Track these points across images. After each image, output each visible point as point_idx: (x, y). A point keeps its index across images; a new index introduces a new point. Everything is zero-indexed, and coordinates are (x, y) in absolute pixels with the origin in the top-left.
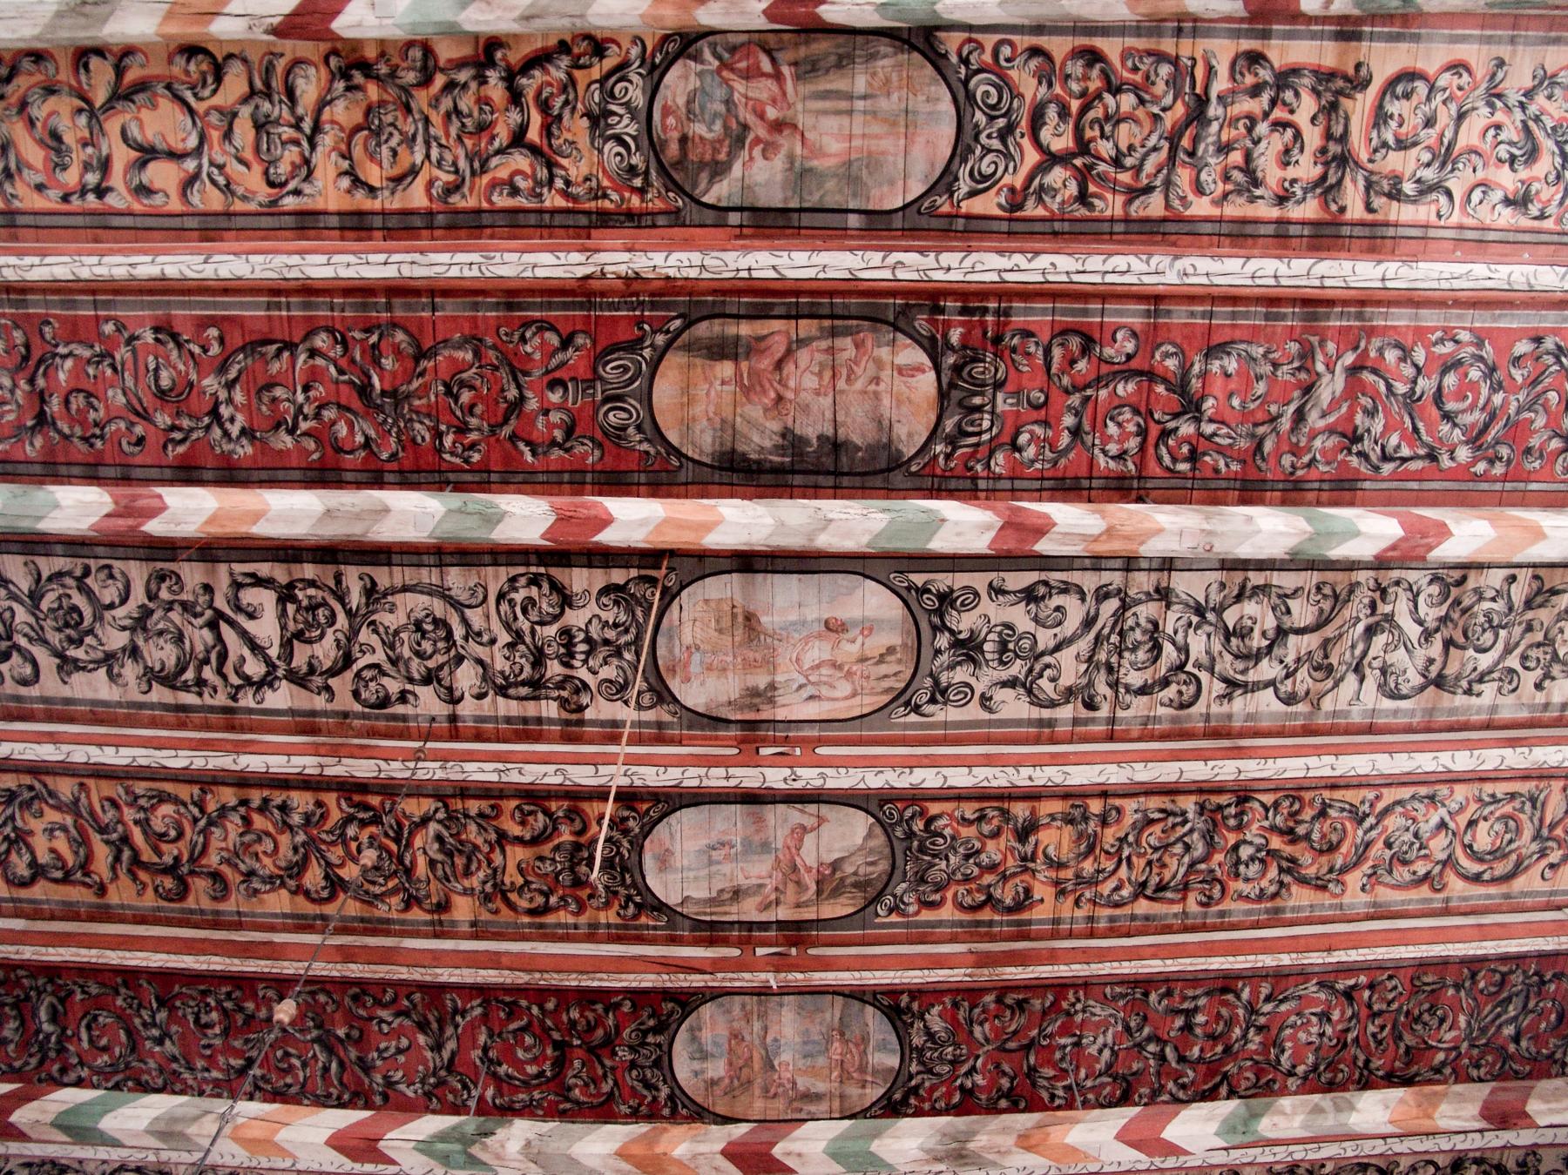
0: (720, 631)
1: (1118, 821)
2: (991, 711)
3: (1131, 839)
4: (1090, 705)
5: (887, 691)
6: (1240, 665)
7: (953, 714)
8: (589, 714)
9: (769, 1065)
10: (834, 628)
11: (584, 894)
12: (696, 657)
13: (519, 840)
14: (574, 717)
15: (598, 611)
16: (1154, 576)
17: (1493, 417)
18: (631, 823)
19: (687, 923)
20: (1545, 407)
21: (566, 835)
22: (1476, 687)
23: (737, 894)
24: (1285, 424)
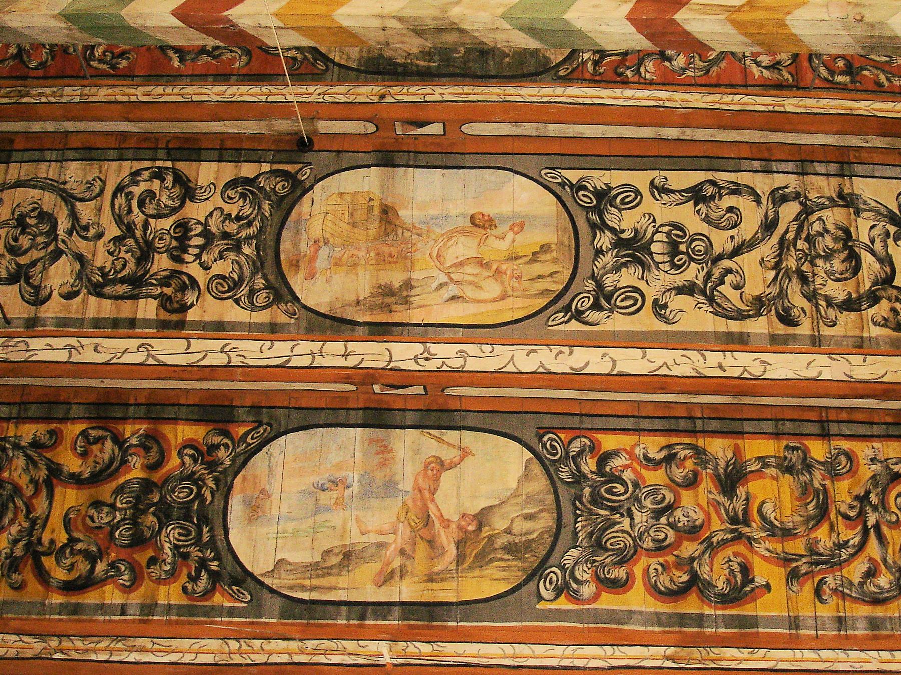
0: (354, 225)
1: (852, 472)
2: (668, 322)
3: (874, 498)
4: (787, 319)
5: (542, 293)
7: (619, 323)
8: (192, 315)
10: (481, 224)
11: (142, 557)
12: (324, 252)
13: (76, 480)
14: (174, 317)
15: (221, 204)
16: (834, 181)
18: (222, 453)
19: (278, 602)
21: (136, 472)
23: (349, 557)
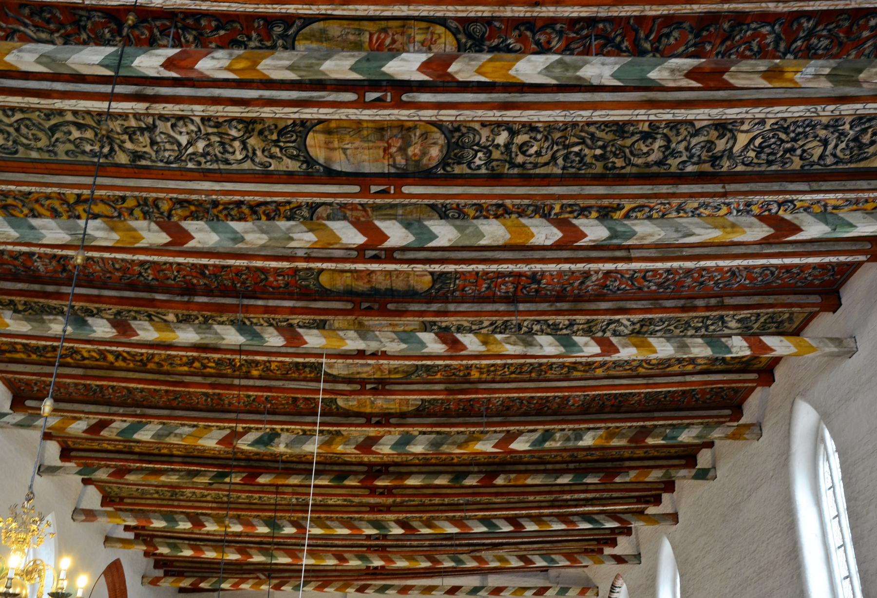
23: (358, 373)
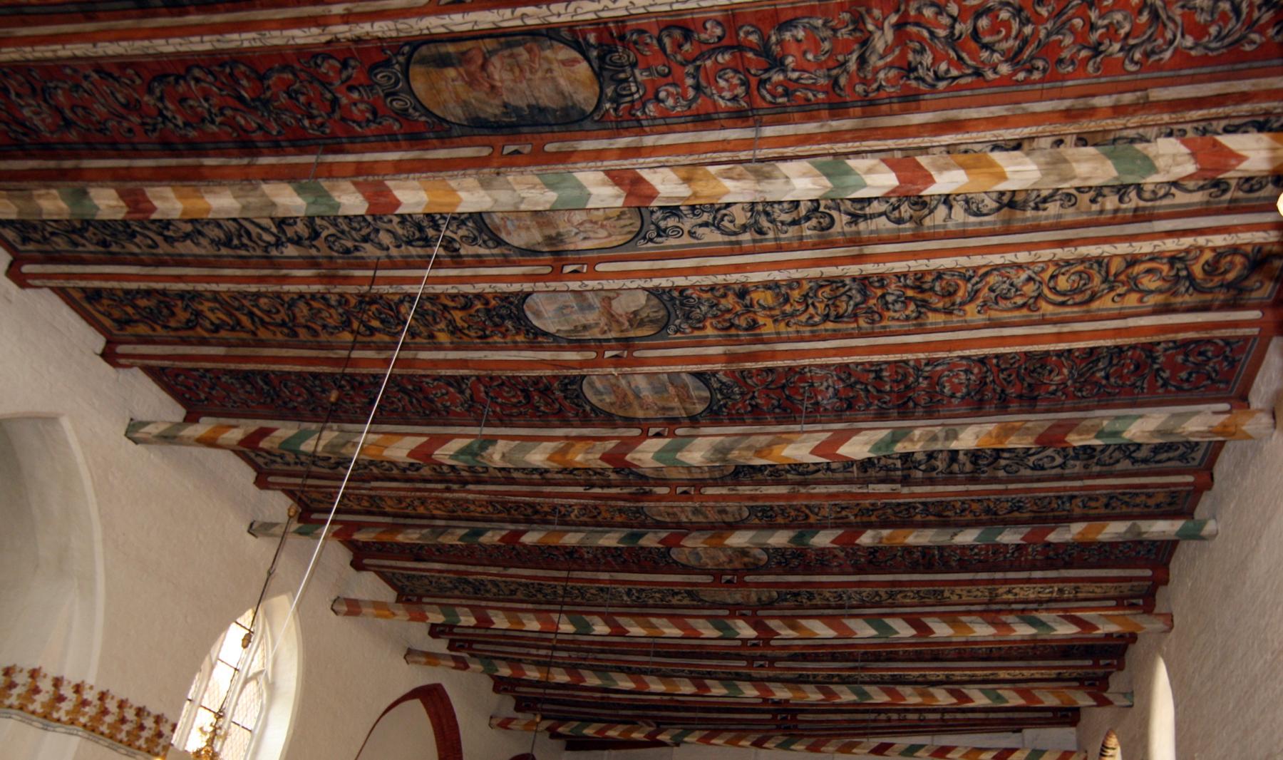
4: (761, 232)
5: (630, 232)
6: (859, 206)
7: (672, 242)
9: (638, 396)
11: (503, 329)
17: (1025, 42)
20: (1072, 30)
22: (1041, 206)
23: (585, 327)
24: (852, 65)
